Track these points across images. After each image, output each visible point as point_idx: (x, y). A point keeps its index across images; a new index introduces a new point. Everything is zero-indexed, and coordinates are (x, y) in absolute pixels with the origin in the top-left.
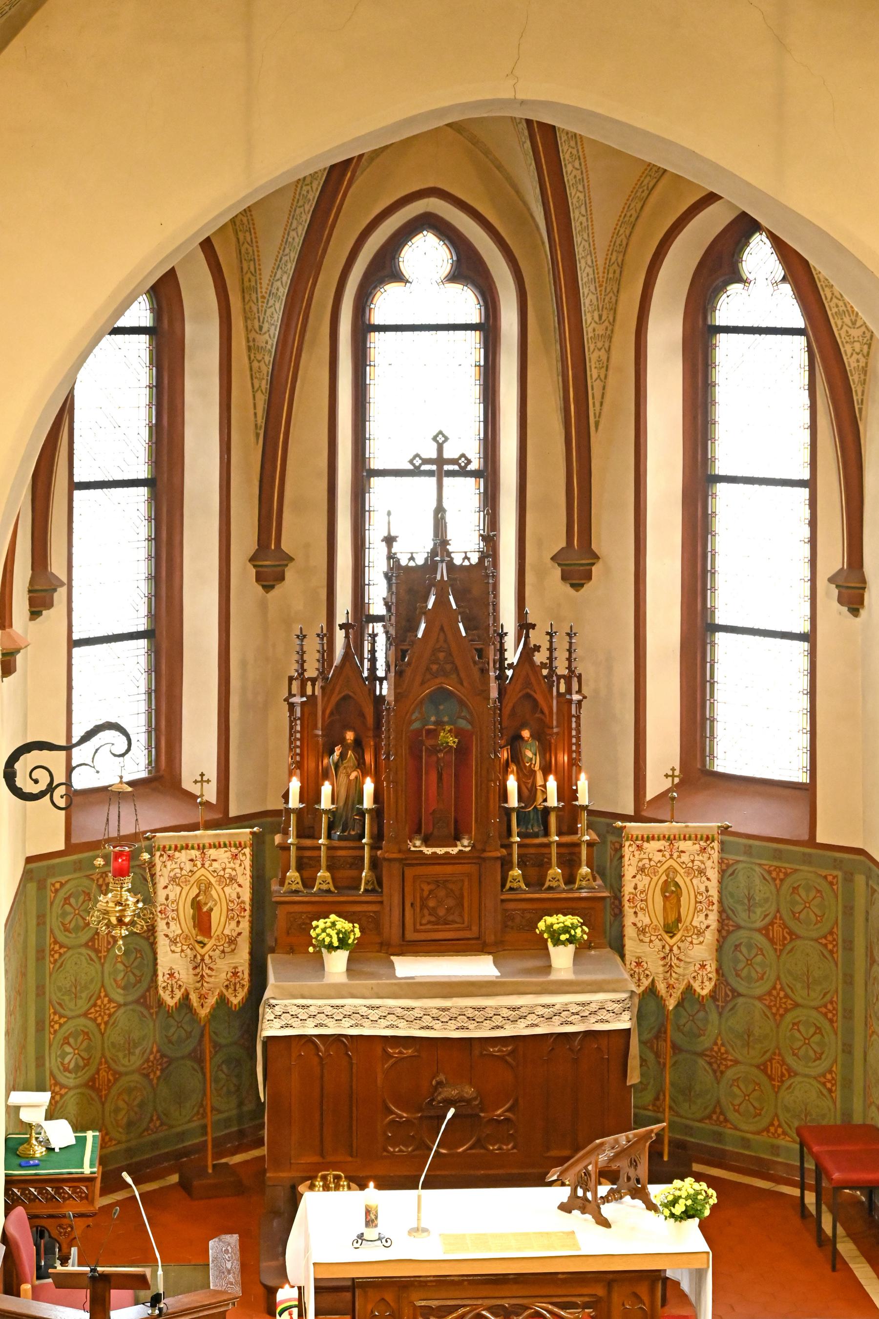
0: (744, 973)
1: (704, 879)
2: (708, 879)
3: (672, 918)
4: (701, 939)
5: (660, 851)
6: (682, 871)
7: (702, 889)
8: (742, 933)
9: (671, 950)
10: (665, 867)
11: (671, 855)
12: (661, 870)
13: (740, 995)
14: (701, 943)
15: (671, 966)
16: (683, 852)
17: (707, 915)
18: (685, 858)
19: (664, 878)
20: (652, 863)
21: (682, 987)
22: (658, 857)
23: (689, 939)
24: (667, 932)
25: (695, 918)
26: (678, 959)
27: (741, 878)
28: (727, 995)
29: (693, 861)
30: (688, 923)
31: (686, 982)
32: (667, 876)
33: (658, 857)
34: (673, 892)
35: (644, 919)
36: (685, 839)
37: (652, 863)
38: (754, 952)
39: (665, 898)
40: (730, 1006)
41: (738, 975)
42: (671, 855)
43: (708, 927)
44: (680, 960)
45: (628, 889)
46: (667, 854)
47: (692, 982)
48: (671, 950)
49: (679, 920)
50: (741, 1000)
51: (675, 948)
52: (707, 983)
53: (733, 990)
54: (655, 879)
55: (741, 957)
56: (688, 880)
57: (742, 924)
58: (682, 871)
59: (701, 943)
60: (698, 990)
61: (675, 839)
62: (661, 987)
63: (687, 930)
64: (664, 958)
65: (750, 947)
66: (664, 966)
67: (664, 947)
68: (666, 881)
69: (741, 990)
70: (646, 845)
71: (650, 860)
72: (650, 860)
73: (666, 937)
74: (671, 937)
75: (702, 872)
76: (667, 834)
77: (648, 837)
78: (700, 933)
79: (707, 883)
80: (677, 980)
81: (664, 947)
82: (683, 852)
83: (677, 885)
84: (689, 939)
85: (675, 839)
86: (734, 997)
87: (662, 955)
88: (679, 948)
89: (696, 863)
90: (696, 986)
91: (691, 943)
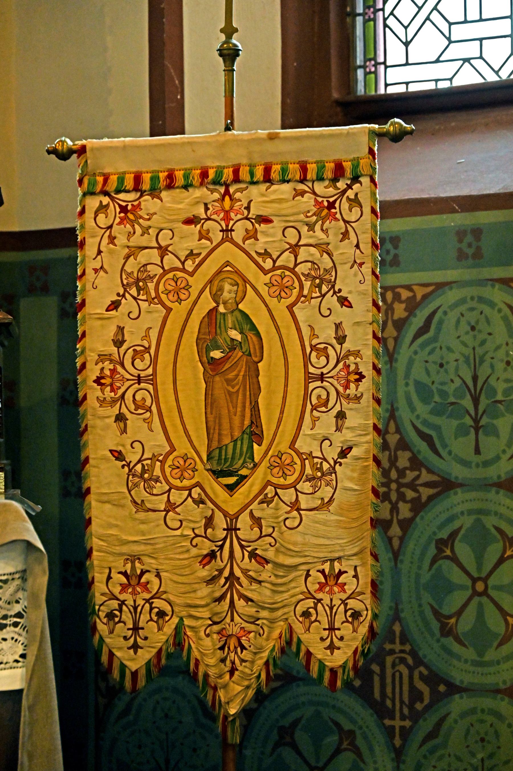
0: (465, 624)
1: (331, 300)
2: (344, 302)
3: (236, 423)
4: (326, 492)
5: (190, 221)
6: (261, 281)
7: (328, 334)
8: (458, 501)
9: (231, 529)
10: (210, 268)
11: (227, 231)
12: (197, 283)
13: (454, 689)
14: (326, 505)
15: (232, 577)
16: (265, 220)
17: (341, 416)
18: (269, 238)
19: (207, 303)
20: (170, 261)
21: (269, 645)
22: (187, 240)
23: (289, 495)
24: (218, 474)
25: (306, 429)
26: (253, 555)
27: (453, 337)
28: (416, 695)
29: (294, 249)
30: (282, 444)
31: (280, 627)
32: (216, 297)
33: (187, 240)
34: (233, 345)
35: (147, 438)
36: (267, 179)
37: (170, 261)
38: (494, 551)
39: (213, 366)
40: (426, 725)
41: (446, 631)
42: (227, 231)
43: (344, 453)
44: (264, 561)
45: (96, 341)
46: (215, 229)
47: (299, 628)
48: (231, 529)
49: (255, 435)
50: (458, 704)
51: (244, 521)
52: (346, 630)
53: (433, 679)
54: (179, 310)
55: (457, 576)
56: (280, 308)
57: (457, 472)
58: (261, 281)
59: (326, 505)
60: (319, 652)
61: (237, 180)
62: (204, 649)
63: (280, 465)
64: (212, 555)
65: (480, 538)
66: (212, 580)
67: (209, 522)
68: (213, 312)
69: (459, 674)
70: (148, 203)
71: (163, 251)
72: (163, 251)
73: (216, 489)
74: (231, 488)
75: (323, 280)
76: (212, 164)
77: (155, 179)
78: (322, 475)
79: (342, 314)
80: (254, 621)
81: (209, 522)
82: (265, 220)
83: (246, 322)
84: (289, 495)
85: (237, 180)
86: (437, 698)
87: (207, 547)
88: (257, 521)
89: (303, 254)
90: (313, 640)
91: (295, 506)
